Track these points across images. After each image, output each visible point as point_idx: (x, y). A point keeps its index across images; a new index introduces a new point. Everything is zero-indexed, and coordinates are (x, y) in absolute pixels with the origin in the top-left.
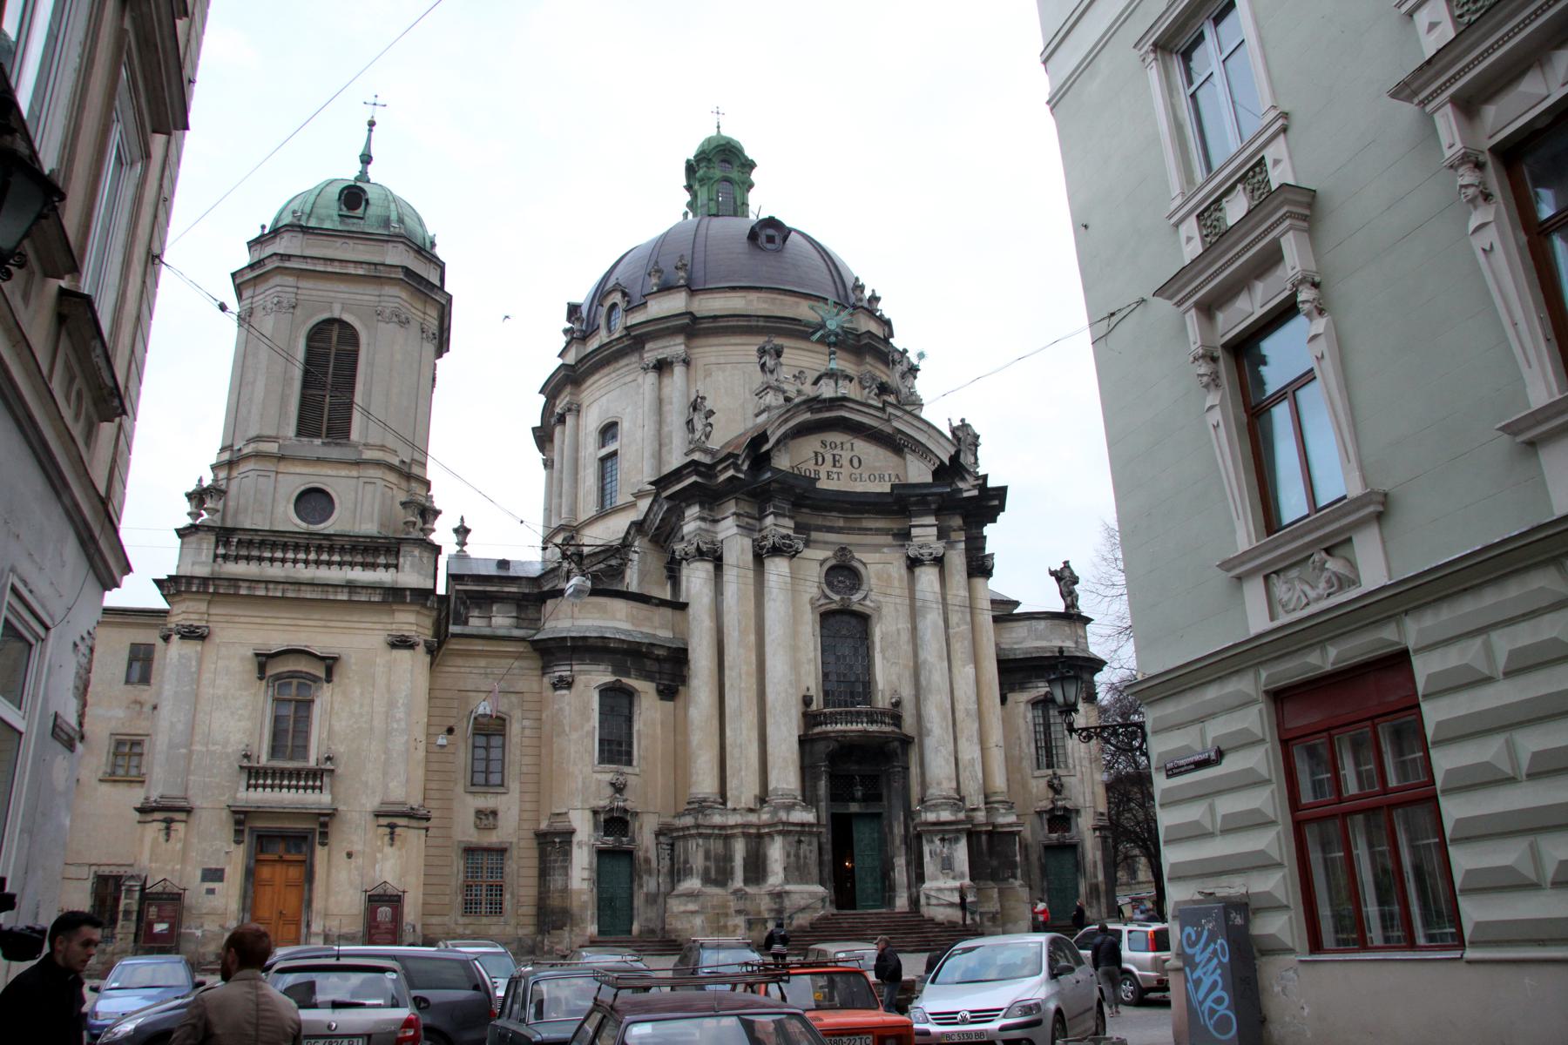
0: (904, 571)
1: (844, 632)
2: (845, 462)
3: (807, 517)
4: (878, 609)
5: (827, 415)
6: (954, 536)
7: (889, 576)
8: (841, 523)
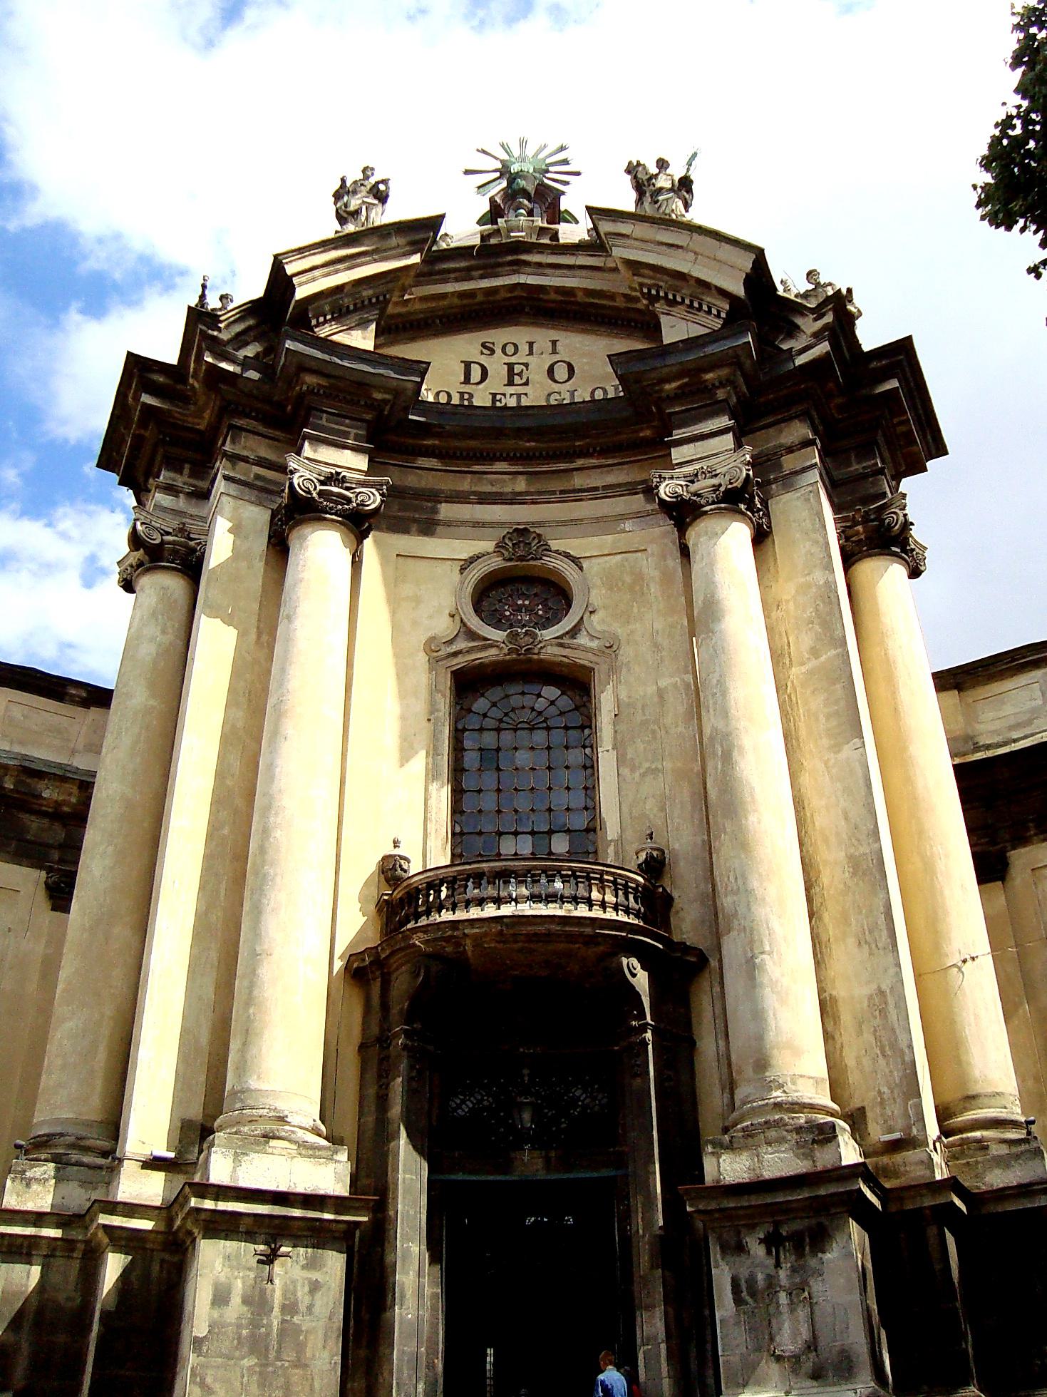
0: (674, 562)
1: (526, 715)
2: (537, 373)
3: (426, 474)
4: (611, 648)
5: (485, 284)
6: (789, 462)
7: (639, 577)
8: (521, 485)
